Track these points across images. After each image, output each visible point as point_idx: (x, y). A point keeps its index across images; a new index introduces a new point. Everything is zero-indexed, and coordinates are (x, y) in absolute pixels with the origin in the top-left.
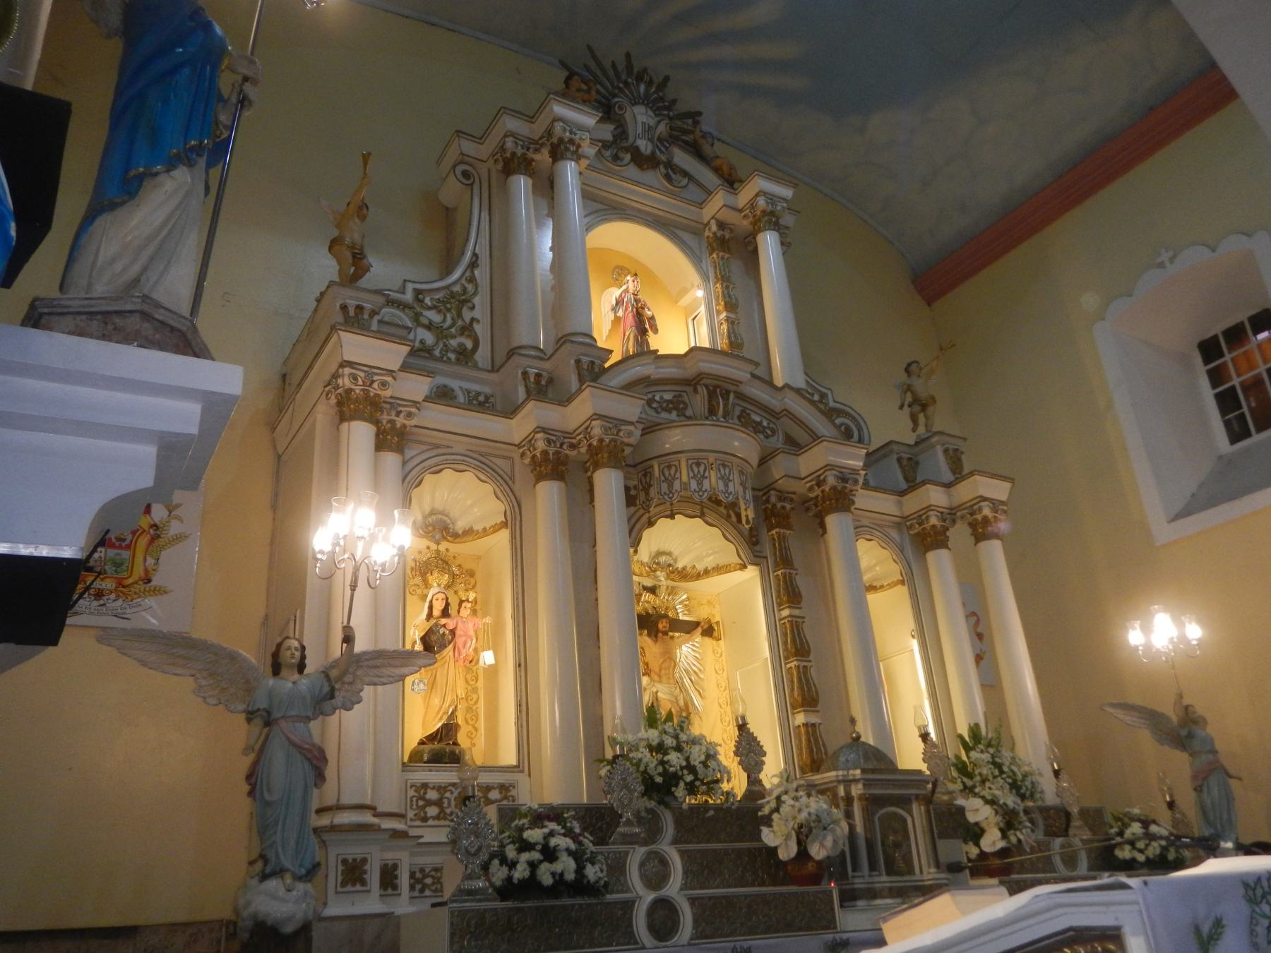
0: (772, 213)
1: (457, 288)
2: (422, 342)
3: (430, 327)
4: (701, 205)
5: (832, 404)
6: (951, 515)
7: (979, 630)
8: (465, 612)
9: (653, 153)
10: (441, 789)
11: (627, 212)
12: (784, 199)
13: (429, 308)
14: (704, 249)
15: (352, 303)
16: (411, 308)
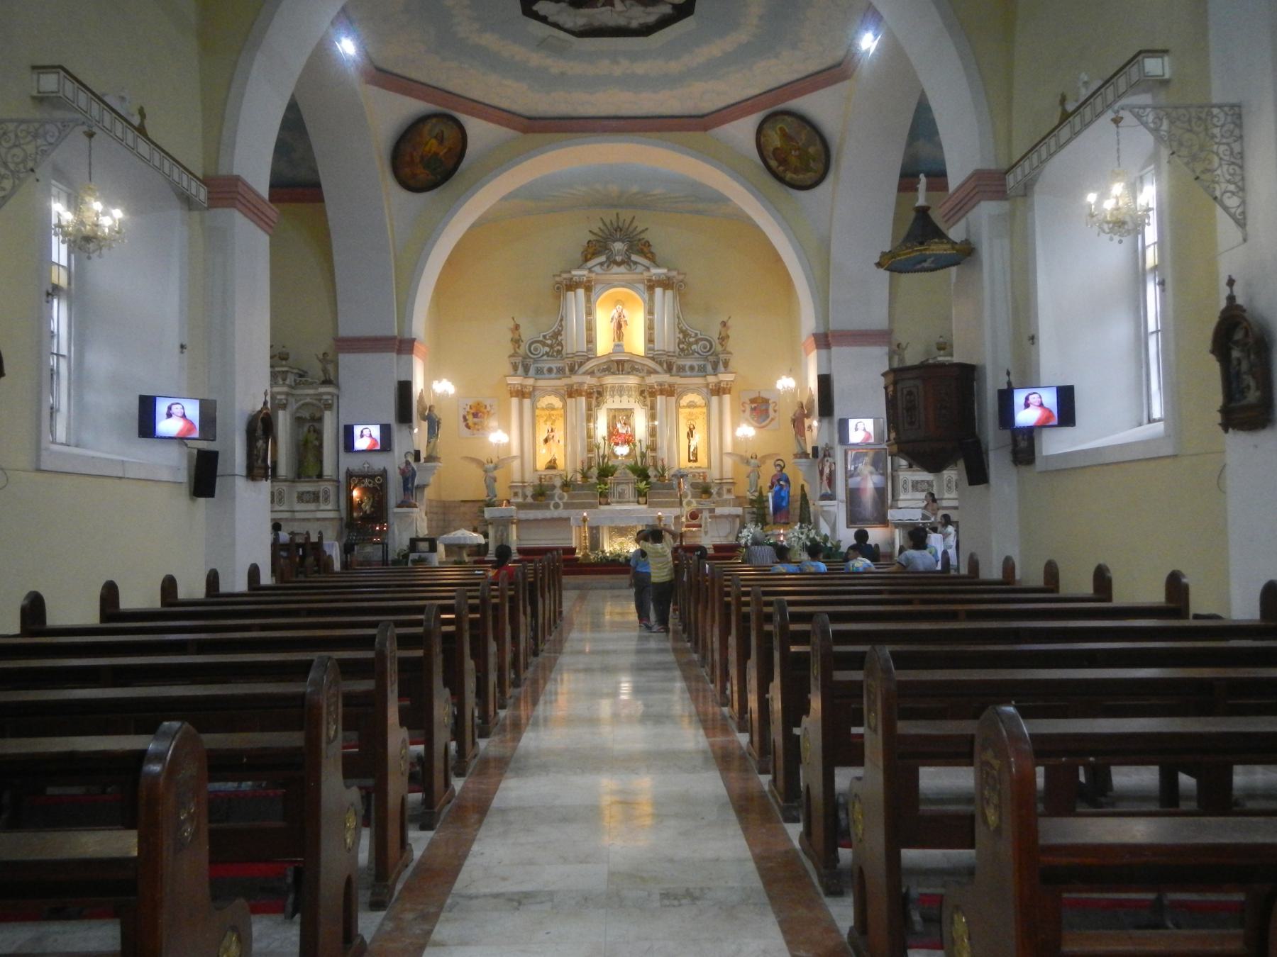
0: (659, 281)
1: (556, 330)
2: (546, 352)
3: (548, 346)
4: (642, 274)
5: (700, 336)
6: (719, 383)
7: (776, 408)
8: (556, 431)
9: (622, 260)
10: (545, 475)
11: (616, 283)
12: (663, 274)
13: (548, 340)
14: (646, 290)
15: (513, 362)
16: (542, 341)
